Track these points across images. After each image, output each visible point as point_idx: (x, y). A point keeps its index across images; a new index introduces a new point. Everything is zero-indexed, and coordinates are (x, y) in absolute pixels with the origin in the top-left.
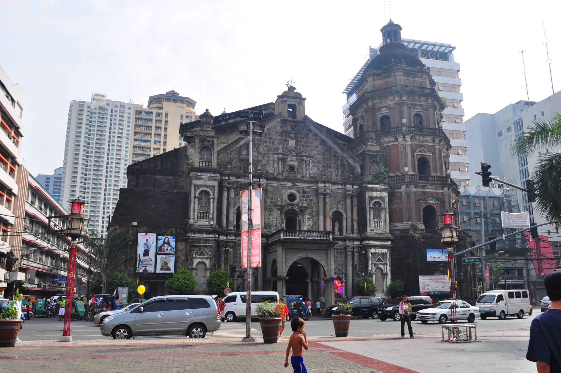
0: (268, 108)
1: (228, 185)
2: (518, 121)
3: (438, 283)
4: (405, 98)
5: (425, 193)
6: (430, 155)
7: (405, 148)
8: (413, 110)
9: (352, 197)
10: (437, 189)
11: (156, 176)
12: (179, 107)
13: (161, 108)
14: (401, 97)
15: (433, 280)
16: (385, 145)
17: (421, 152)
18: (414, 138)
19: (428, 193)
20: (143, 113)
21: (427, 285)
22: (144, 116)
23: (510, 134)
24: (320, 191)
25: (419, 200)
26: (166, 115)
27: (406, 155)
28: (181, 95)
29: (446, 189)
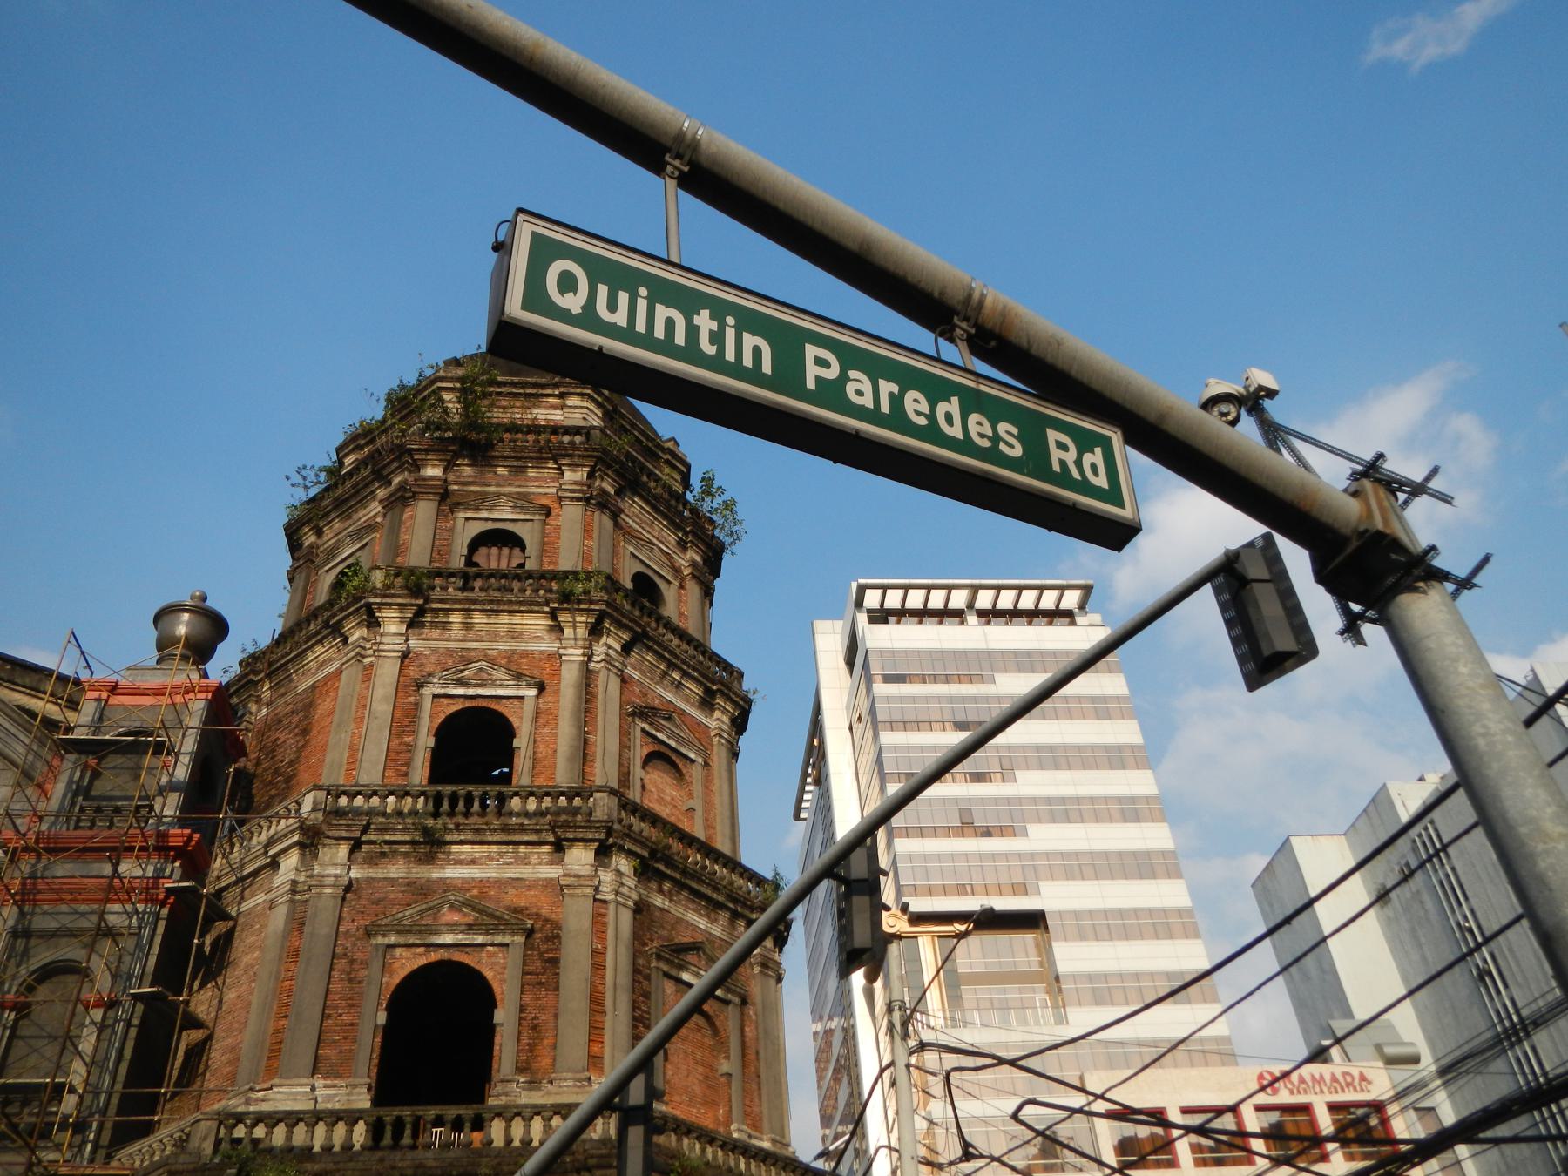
4: (433, 471)
5: (421, 890)
6: (522, 698)
7: (368, 674)
8: (469, 515)
10: (525, 861)
14: (416, 467)
16: (300, 689)
17: (461, 683)
18: (434, 625)
19: (446, 886)
23: (1414, 889)
25: (369, 934)
27: (364, 706)
29: (580, 858)
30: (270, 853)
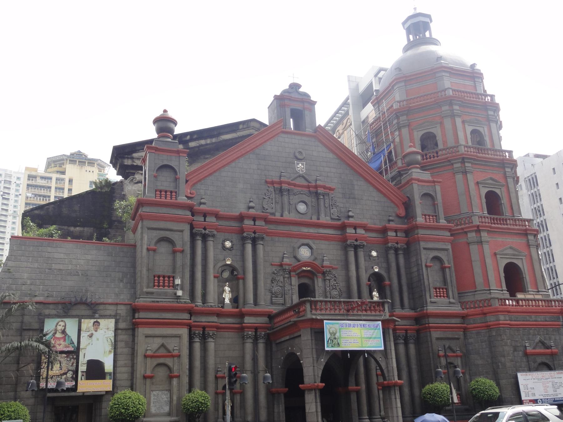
0: (248, 128)
1: (203, 231)
2: (530, 178)
3: (548, 385)
9: (396, 250)
11: (72, 229)
12: (88, 171)
13: (63, 173)
14: (451, 104)
15: (538, 379)
20: (38, 179)
21: (531, 388)
22: (40, 182)
24: (349, 242)
26: (69, 181)
28: (90, 157)
29: (531, 238)
30: (465, 230)
